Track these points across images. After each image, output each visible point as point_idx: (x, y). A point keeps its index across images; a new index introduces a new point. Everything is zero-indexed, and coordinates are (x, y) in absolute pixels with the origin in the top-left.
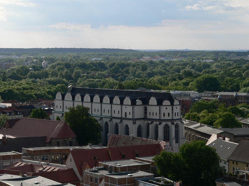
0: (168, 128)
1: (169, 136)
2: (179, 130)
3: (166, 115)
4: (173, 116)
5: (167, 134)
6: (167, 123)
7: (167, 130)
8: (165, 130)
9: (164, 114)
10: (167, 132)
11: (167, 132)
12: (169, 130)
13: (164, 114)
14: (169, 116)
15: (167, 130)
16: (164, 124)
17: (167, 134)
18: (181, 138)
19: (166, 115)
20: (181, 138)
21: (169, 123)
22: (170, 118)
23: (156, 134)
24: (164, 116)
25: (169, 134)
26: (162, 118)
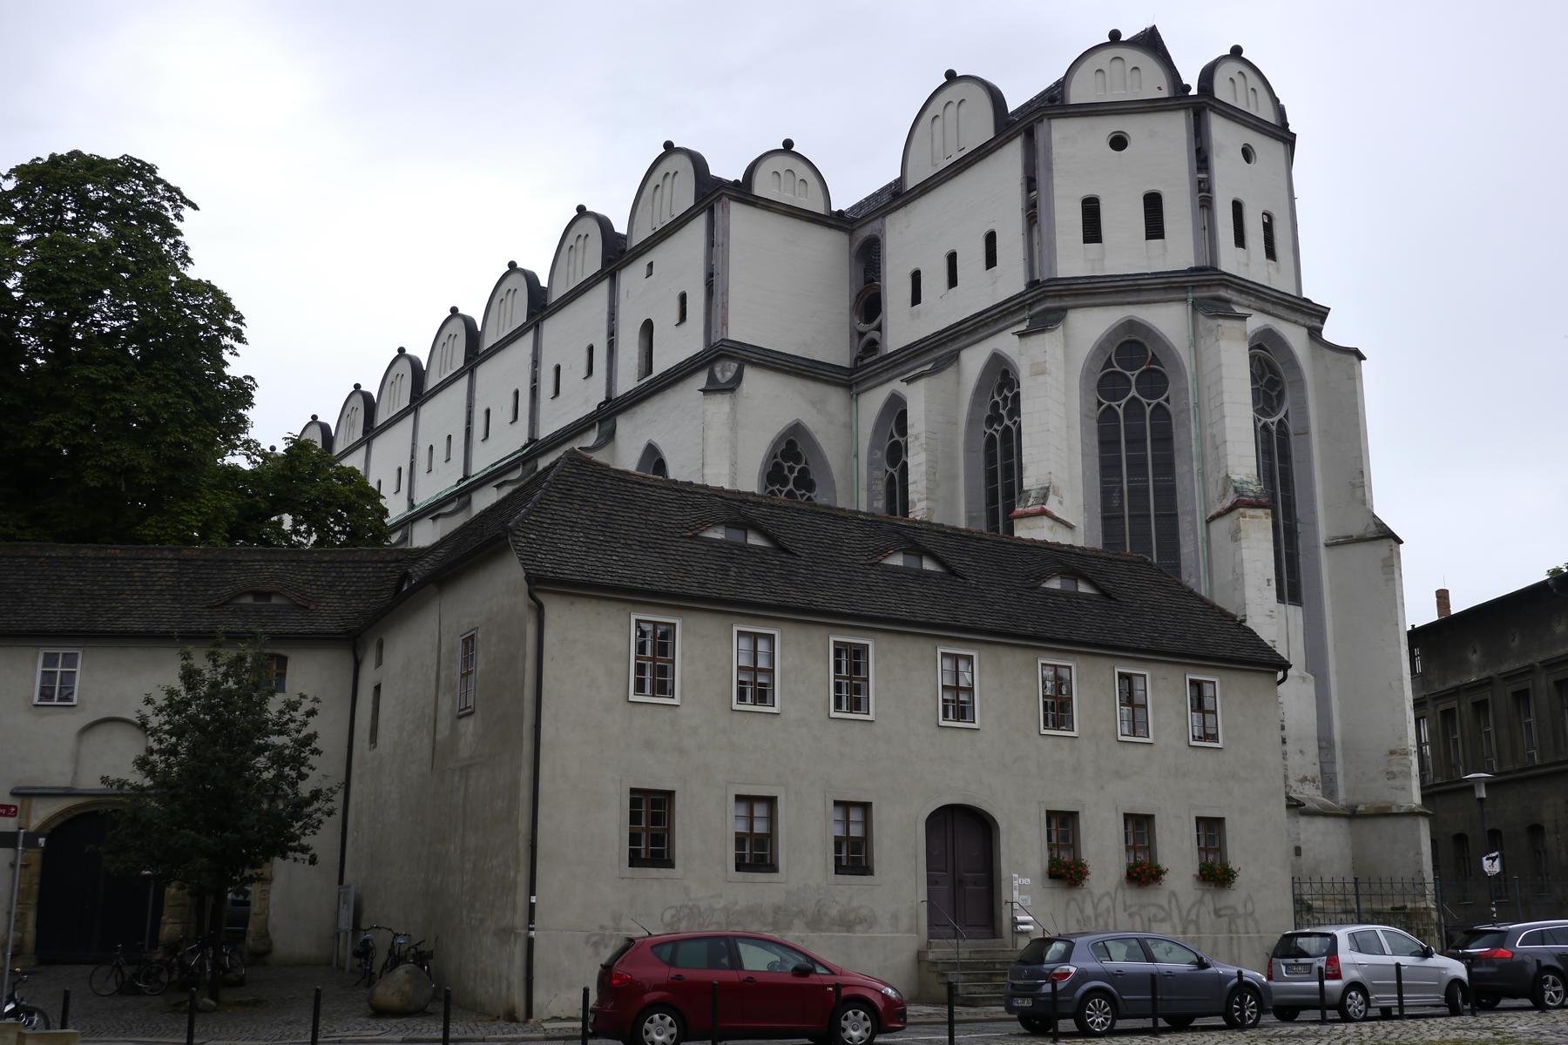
1: (1167, 493)
2: (1305, 432)
5: (1137, 466)
6: (1130, 325)
10: (1136, 441)
11: (1136, 441)
12: (1162, 413)
14: (1155, 229)
15: (1134, 407)
16: (1091, 326)
17: (1137, 466)
18: (1332, 545)
19: (1123, 218)
21: (1168, 320)
22: (1177, 251)
23: (991, 477)
24: (1092, 230)
25: (1166, 466)
26: (1072, 259)
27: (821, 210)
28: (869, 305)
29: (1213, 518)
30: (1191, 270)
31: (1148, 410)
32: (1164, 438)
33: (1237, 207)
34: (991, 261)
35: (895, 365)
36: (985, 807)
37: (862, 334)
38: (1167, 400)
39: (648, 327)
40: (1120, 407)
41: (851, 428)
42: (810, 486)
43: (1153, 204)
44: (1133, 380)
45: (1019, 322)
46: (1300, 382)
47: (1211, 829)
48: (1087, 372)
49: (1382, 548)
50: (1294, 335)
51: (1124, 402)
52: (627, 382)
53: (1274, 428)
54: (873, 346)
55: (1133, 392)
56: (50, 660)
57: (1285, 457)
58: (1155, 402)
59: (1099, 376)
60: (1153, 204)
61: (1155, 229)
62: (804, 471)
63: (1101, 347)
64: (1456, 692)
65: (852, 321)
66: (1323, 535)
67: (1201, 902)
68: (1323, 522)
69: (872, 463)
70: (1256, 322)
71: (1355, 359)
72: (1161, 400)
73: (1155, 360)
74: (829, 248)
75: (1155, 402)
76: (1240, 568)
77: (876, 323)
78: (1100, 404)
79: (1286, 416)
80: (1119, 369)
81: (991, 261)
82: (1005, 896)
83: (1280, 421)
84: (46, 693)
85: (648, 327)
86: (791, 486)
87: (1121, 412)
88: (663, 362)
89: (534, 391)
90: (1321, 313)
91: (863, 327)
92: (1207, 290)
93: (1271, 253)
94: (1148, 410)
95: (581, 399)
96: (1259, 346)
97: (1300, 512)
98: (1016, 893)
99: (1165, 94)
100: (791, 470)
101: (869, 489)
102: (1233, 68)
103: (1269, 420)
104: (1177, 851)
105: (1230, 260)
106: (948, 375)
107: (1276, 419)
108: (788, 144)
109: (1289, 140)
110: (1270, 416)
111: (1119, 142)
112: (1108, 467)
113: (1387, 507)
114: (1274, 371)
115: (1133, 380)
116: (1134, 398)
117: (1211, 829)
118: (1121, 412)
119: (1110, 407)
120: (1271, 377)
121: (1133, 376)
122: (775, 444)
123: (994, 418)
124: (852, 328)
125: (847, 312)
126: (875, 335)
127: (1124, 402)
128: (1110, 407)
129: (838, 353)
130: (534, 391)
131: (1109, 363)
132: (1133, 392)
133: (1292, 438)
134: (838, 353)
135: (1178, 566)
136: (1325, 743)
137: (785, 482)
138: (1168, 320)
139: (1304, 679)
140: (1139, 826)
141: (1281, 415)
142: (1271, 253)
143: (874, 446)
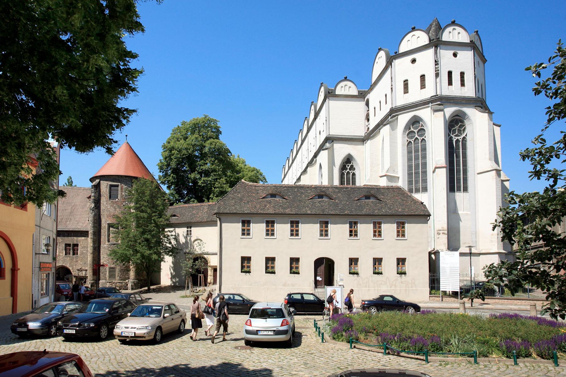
3: (415, 84)
5: (417, 158)
10: (417, 151)
11: (417, 151)
13: (406, 83)
17: (417, 158)
25: (424, 157)
32: (424, 149)
42: (354, 169)
55: (416, 136)
62: (352, 166)
67: (397, 280)
79: (466, 135)
83: (464, 138)
87: (413, 142)
100: (348, 166)
103: (459, 138)
107: (462, 137)
110: (459, 136)
112: (410, 159)
128: (410, 142)
137: (347, 169)
141: (464, 135)
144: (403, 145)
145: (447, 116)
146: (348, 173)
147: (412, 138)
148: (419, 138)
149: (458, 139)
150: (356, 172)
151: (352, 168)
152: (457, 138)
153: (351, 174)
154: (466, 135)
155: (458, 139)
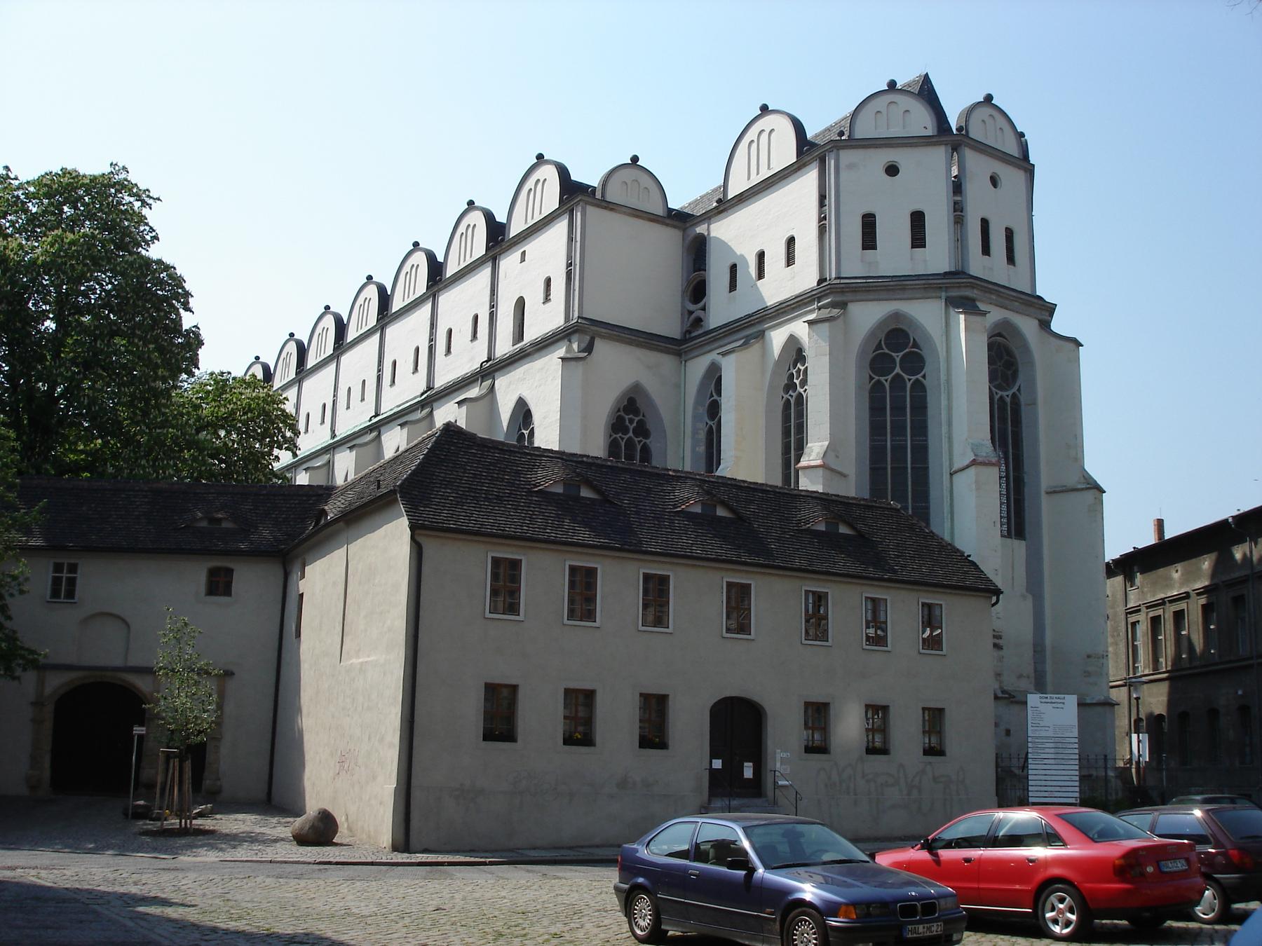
0: (915, 362)
1: (921, 452)
2: (1034, 403)
4: (960, 241)
5: (899, 429)
6: (896, 316)
7: (898, 382)
8: (876, 389)
9: (869, 223)
10: (898, 409)
11: (898, 409)
12: (919, 387)
14: (918, 240)
15: (898, 382)
17: (899, 429)
18: (1052, 492)
19: (894, 231)
20: (1052, 492)
21: (926, 314)
25: (921, 429)
26: (856, 265)
27: (660, 211)
28: (698, 291)
29: (956, 472)
30: (946, 275)
31: (909, 385)
32: (920, 407)
33: (985, 224)
34: (790, 260)
35: (715, 340)
36: (756, 698)
37: (691, 313)
38: (924, 377)
39: (520, 304)
40: (886, 381)
41: (679, 387)
43: (918, 220)
44: (898, 360)
45: (811, 311)
46: (1031, 363)
47: (934, 718)
48: (862, 352)
49: (1090, 496)
50: (1027, 325)
51: (890, 377)
52: (504, 347)
53: (1008, 400)
54: (698, 321)
55: (898, 370)
56: (58, 568)
57: (1017, 422)
58: (914, 378)
59: (871, 356)
60: (918, 220)
61: (918, 240)
62: (641, 424)
63: (873, 333)
64: (1162, 602)
65: (683, 303)
66: (1045, 481)
68: (1046, 473)
69: (696, 418)
70: (996, 315)
71: (1072, 345)
72: (919, 376)
73: (916, 345)
74: (668, 241)
75: (914, 378)
76: (969, 511)
77: (701, 304)
78: (871, 379)
79: (1019, 390)
80: (886, 351)
81: (790, 260)
82: (770, 766)
83: (1014, 395)
84: (55, 593)
85: (520, 304)
86: (631, 434)
87: (887, 385)
88: (531, 334)
89: (431, 349)
90: (1051, 309)
91: (692, 307)
92: (958, 289)
93: (1011, 259)
94: (909, 385)
95: (465, 358)
96: (999, 335)
97: (1026, 468)
98: (778, 765)
99: (929, 132)
100: (631, 421)
101: (693, 438)
102: (986, 111)
103: (1005, 394)
104: (907, 733)
105: (977, 265)
106: (755, 348)
107: (1010, 393)
108: (635, 159)
109: (1029, 170)
110: (1006, 390)
111: (892, 170)
112: (876, 428)
113: (1095, 465)
114: (1009, 353)
115: (898, 360)
116: (898, 375)
117: (934, 718)
118: (887, 385)
119: (879, 381)
120: (1005, 360)
121: (898, 356)
122: (619, 400)
123: (790, 386)
124: (683, 307)
125: (680, 294)
126: (700, 313)
127: (890, 377)
128: (879, 381)
129: (671, 327)
130: (431, 349)
131: (879, 347)
132: (898, 370)
133: (1023, 407)
134: (671, 327)
135: (928, 508)
136: (1039, 649)
137: (626, 431)
138: (926, 314)
139: (1024, 597)
140: (878, 712)
141: (1015, 390)
142: (1011, 259)
143: (697, 403)
144: (859, 388)
145: (988, 326)
146: (630, 444)
147: (884, 373)
148: (906, 377)
149: (1001, 397)
150: (653, 443)
151: (642, 430)
152: (1000, 393)
153: (639, 448)
154: (1019, 390)
155: (1001, 397)
